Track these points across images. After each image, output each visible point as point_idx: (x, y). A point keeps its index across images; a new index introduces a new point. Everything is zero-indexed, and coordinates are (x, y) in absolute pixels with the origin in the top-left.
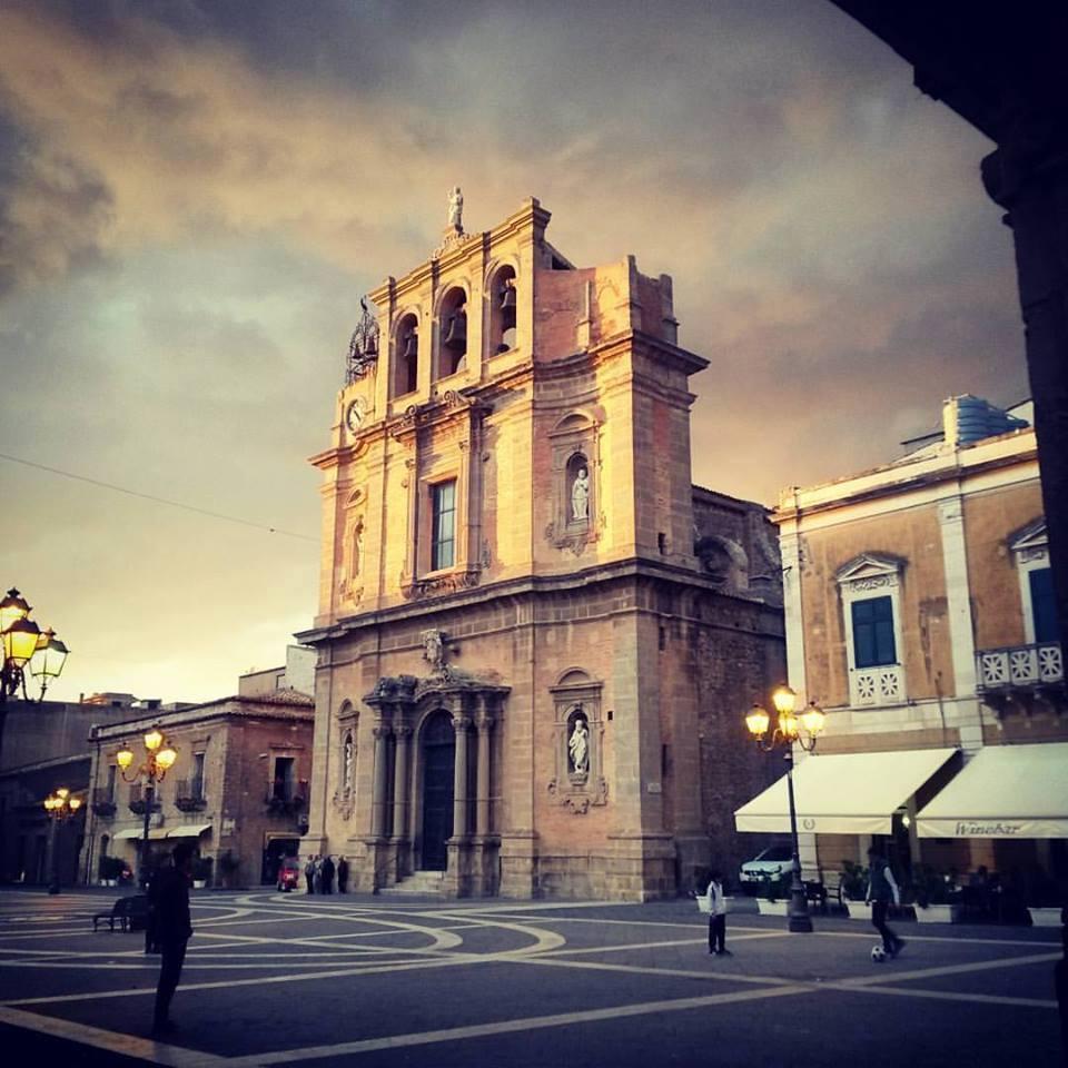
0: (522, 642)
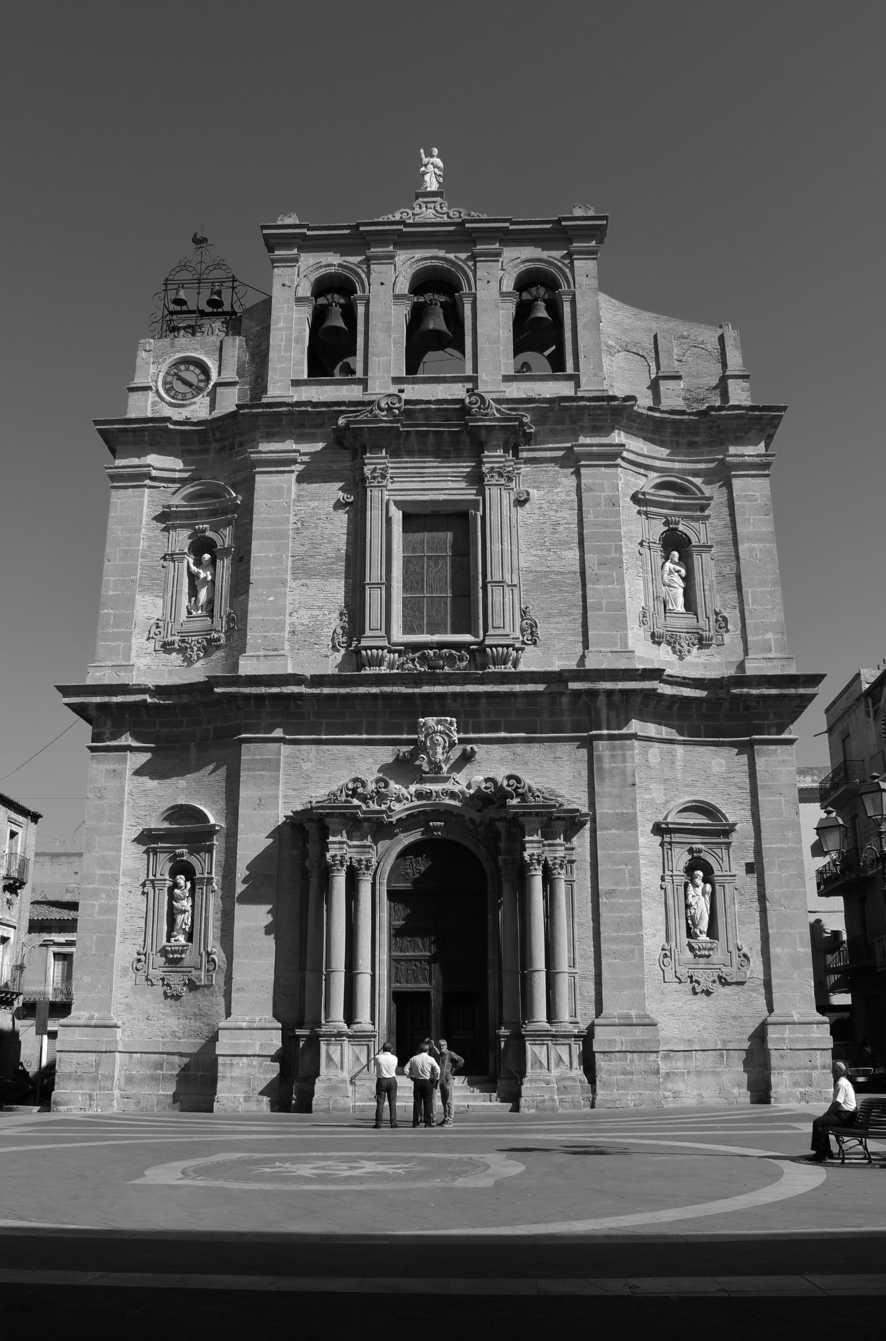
0: (612, 756)
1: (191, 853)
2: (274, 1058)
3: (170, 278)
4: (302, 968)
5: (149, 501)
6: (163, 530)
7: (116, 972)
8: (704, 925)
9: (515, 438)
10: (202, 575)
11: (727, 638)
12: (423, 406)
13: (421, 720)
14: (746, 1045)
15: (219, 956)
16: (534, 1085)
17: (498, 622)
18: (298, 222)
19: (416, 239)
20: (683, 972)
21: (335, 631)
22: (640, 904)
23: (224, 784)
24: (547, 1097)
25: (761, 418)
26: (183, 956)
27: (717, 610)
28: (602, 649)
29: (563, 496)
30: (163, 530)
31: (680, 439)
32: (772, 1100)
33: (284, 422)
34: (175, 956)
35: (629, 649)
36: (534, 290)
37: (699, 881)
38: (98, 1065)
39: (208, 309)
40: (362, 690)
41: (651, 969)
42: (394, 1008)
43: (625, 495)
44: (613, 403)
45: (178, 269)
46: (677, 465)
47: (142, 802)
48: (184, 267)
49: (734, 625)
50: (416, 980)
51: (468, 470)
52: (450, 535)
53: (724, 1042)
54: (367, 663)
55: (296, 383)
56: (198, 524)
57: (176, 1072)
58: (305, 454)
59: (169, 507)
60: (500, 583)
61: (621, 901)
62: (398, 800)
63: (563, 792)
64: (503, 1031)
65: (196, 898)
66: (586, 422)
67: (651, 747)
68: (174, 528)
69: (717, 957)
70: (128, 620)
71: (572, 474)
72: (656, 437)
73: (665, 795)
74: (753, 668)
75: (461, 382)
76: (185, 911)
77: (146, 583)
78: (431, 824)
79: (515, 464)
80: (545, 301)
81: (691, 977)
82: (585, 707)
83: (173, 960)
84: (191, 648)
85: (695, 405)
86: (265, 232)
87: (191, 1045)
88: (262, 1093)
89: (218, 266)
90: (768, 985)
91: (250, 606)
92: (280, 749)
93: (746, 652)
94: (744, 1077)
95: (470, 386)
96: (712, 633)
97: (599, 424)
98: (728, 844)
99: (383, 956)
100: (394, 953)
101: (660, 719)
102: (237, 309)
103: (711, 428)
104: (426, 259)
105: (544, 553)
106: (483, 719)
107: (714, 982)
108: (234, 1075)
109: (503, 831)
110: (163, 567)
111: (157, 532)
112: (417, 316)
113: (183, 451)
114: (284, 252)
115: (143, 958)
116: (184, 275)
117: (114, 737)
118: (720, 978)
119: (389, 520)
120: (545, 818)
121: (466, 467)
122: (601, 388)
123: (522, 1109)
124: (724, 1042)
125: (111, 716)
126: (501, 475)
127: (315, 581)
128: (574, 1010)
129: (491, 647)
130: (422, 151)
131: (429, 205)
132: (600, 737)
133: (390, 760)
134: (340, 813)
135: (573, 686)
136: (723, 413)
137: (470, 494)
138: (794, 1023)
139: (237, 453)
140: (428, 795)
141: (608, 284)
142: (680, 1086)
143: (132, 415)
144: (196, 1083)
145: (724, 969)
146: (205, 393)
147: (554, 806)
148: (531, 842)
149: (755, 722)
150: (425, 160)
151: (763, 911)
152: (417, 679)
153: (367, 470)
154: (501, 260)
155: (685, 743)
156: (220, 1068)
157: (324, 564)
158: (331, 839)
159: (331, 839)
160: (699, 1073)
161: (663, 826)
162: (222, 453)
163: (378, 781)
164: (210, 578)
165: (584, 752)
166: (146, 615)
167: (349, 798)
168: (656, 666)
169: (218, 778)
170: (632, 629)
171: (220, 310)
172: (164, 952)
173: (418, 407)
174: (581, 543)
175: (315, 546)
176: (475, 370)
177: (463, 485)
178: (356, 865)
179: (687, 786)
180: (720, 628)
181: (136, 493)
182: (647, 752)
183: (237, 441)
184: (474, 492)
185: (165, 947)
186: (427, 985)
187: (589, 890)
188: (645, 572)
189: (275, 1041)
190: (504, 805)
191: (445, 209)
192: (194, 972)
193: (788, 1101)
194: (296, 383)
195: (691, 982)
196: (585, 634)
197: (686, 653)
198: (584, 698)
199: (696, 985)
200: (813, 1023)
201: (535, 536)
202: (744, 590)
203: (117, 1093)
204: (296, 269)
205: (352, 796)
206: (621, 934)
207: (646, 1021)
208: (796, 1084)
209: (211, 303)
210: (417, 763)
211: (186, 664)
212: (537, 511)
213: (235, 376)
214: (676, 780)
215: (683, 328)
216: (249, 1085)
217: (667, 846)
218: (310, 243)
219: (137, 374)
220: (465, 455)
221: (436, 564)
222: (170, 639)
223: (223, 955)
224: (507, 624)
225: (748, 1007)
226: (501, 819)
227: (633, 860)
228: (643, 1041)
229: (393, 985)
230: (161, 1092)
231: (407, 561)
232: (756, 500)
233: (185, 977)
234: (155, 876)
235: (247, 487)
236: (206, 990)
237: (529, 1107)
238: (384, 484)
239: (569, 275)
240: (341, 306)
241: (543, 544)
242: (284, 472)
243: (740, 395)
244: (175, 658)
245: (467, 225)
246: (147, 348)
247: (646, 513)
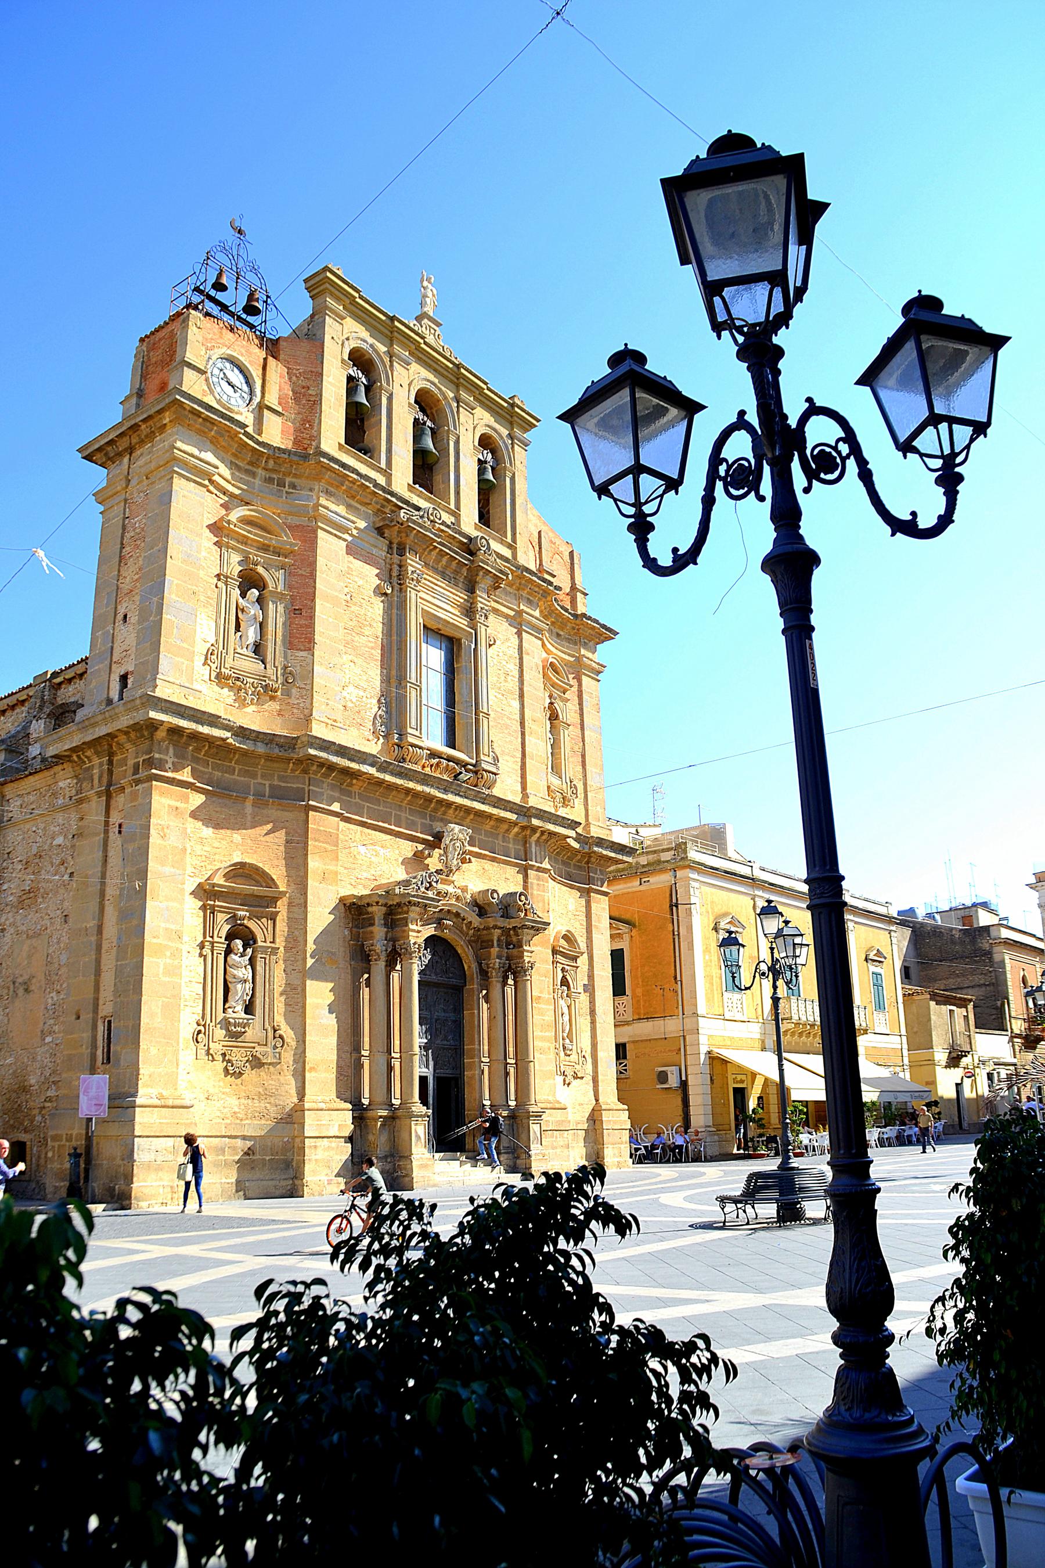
1: (250, 918)
17: (486, 751)
21: (375, 717)
23: (282, 848)
57: (237, 1158)
65: (258, 968)
87: (257, 1128)
88: (338, 1175)
103: (574, 628)
108: (317, 1157)
113: (231, 462)
115: (202, 1028)
129: (486, 771)
133: (410, 855)
157: (366, 646)
158: (411, 927)
169: (277, 840)
172: (226, 1024)
174: (521, 696)
181: (197, 491)
185: (225, 1019)
211: (237, 705)
230: (224, 1180)
234: (212, 937)
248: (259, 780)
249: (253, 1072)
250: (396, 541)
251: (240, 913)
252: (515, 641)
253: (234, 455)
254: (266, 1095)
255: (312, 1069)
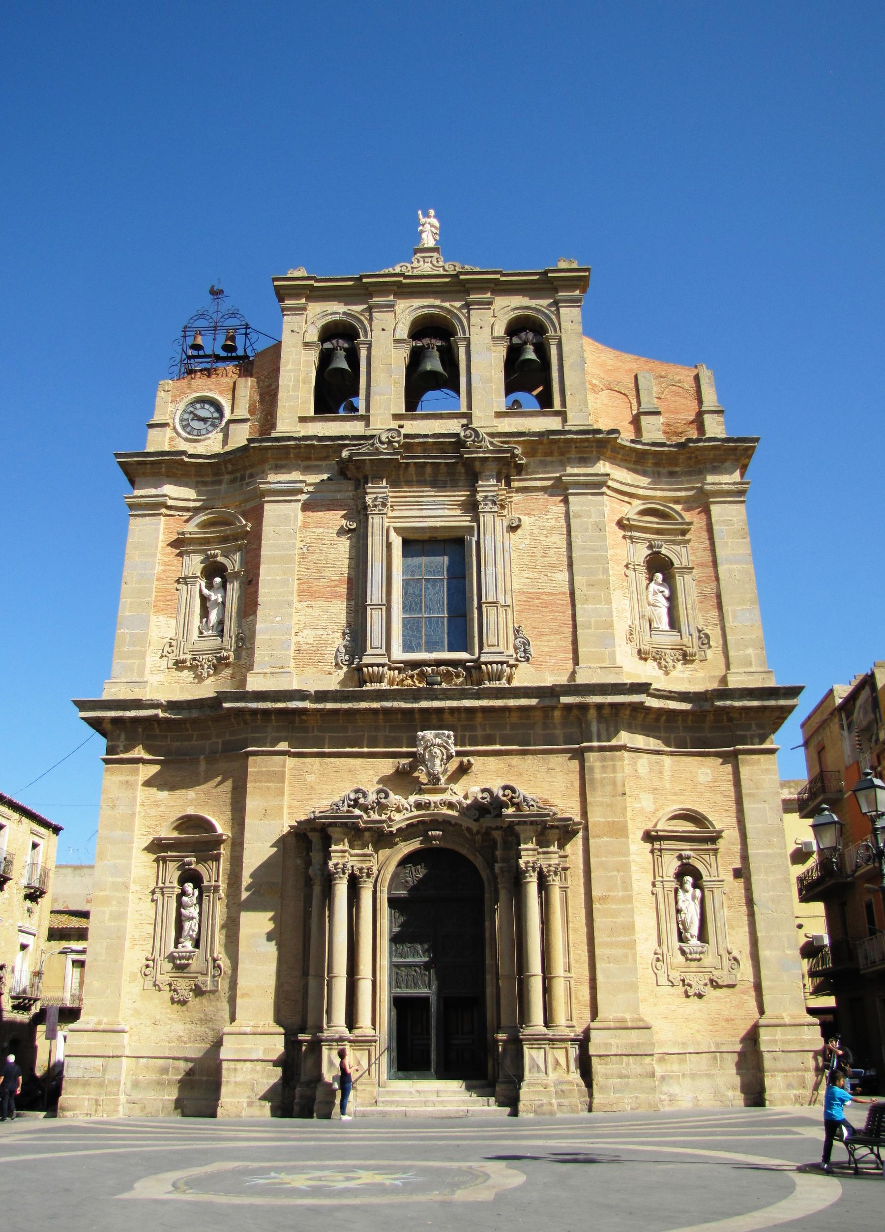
0: (603, 766)
1: (198, 862)
2: (276, 1063)
3: (189, 325)
4: (305, 973)
5: (165, 528)
6: (177, 555)
7: (125, 977)
8: (694, 930)
9: (507, 468)
10: (213, 598)
11: (709, 653)
12: (421, 440)
13: (420, 733)
14: (738, 1047)
15: (224, 962)
16: (532, 1089)
17: (493, 640)
18: (306, 275)
19: (414, 290)
20: (675, 975)
21: (338, 650)
22: (632, 910)
23: (229, 795)
24: (545, 1101)
25: (736, 448)
26: (190, 962)
27: (700, 628)
28: (592, 665)
29: (553, 522)
30: (177, 555)
31: (661, 470)
32: (767, 1102)
33: (292, 455)
34: (183, 962)
35: (617, 665)
36: (523, 335)
37: (688, 886)
38: (105, 1070)
39: (223, 354)
40: (363, 705)
41: (645, 973)
42: (394, 1013)
43: (611, 521)
44: (598, 436)
45: (196, 318)
46: (659, 493)
47: (153, 812)
48: (201, 316)
49: (716, 641)
50: (416, 985)
51: (463, 498)
52: (446, 558)
53: (717, 1044)
54: (367, 678)
55: (303, 420)
56: (210, 550)
57: (179, 1077)
58: (310, 485)
59: (183, 533)
60: (494, 604)
61: (614, 907)
62: (398, 810)
63: (556, 802)
64: (502, 1036)
66: (573, 455)
67: (640, 758)
68: (188, 553)
69: (709, 960)
70: (142, 640)
71: (561, 501)
72: (639, 467)
73: (655, 803)
74: (734, 682)
75: (456, 418)
76: (192, 918)
77: (160, 604)
78: (430, 833)
79: (508, 492)
80: (533, 344)
81: (683, 981)
82: (575, 720)
83: (180, 967)
84: (201, 665)
85: (674, 438)
86: (276, 283)
87: (196, 1050)
88: (264, 1098)
89: (233, 315)
90: (758, 987)
91: (258, 626)
92: (285, 761)
93: (728, 666)
94: (737, 1080)
95: (464, 421)
96: (696, 649)
97: (585, 455)
98: (716, 850)
99: (384, 961)
100: (395, 959)
101: (648, 730)
102: (249, 353)
103: (690, 458)
104: (423, 307)
105: (536, 575)
106: (479, 733)
107: (706, 985)
108: (238, 1079)
109: (499, 840)
110: (177, 590)
111: (172, 558)
112: (416, 358)
113: (197, 482)
114: (293, 302)
115: (151, 963)
116: (202, 323)
117: (127, 750)
118: (712, 981)
119: (389, 546)
120: (539, 827)
121: (461, 495)
122: (587, 423)
123: (520, 1114)
124: (717, 1044)
125: (123, 729)
126: (494, 503)
127: (319, 603)
128: (570, 1016)
129: (486, 663)
130: (420, 212)
131: (426, 260)
132: (591, 749)
134: (342, 823)
135: (564, 700)
136: (701, 444)
137: (465, 521)
138: (785, 1025)
139: (247, 484)
140: (427, 806)
141: (590, 330)
142: (675, 1089)
143: (150, 449)
144: (200, 1088)
145: (715, 972)
146: (219, 429)
147: (548, 815)
148: (527, 850)
149: (739, 733)
150: (423, 220)
151: (751, 915)
152: (416, 695)
153: (369, 499)
154: (492, 308)
155: (672, 754)
156: (224, 1073)
157: (328, 587)
159: (334, 847)
160: (693, 1076)
161: (653, 833)
162: (232, 483)
163: (379, 792)
164: (220, 600)
165: (575, 764)
166: (160, 635)
167: (351, 809)
168: (643, 680)
169: (225, 789)
170: (620, 646)
171: (234, 354)
172: (171, 958)
173: (417, 440)
174: (570, 566)
175: (320, 570)
176: (470, 406)
177: (458, 512)
178: (357, 873)
179: (675, 794)
180: (703, 644)
182: (636, 763)
183: (248, 472)
184: (469, 519)
185: (172, 953)
186: (426, 990)
187: (583, 896)
188: (631, 592)
189: (277, 1045)
190: (500, 815)
191: (441, 263)
192: (201, 978)
193: (782, 1104)
194: (303, 420)
195: (684, 985)
196: (575, 651)
197: (671, 668)
198: (575, 712)
199: (689, 988)
200: (803, 1025)
201: (526, 560)
202: (725, 608)
203: (123, 1098)
204: (304, 316)
205: (354, 807)
206: (614, 939)
207: (641, 1024)
208: (789, 1086)
209: (225, 348)
210: (416, 774)
211: (196, 681)
212: (529, 537)
213: (247, 413)
214: (664, 789)
215: (661, 368)
216: (252, 1089)
217: (657, 853)
218: (318, 293)
219: (156, 412)
220: (461, 484)
221: (434, 586)
222: (182, 657)
223: (228, 961)
224: (501, 642)
225: (739, 1010)
226: (497, 828)
227: (625, 867)
228: (638, 1044)
229: (394, 990)
230: (166, 1097)
231: (406, 583)
232: (733, 525)
233: (192, 983)
234: (164, 883)
235: (256, 515)
236: (212, 996)
237: (527, 1111)
238: (385, 512)
239: (555, 321)
240: (345, 350)
241: (535, 567)
242: (291, 501)
243: (715, 428)
244: (187, 675)
245: (461, 277)
246: (166, 389)
247: (631, 538)
248: (214, 740)
249: (197, 999)
250: (360, 476)
251: (186, 860)
252: (561, 508)
253: (196, 475)
254: (205, 1020)
255: (243, 995)
